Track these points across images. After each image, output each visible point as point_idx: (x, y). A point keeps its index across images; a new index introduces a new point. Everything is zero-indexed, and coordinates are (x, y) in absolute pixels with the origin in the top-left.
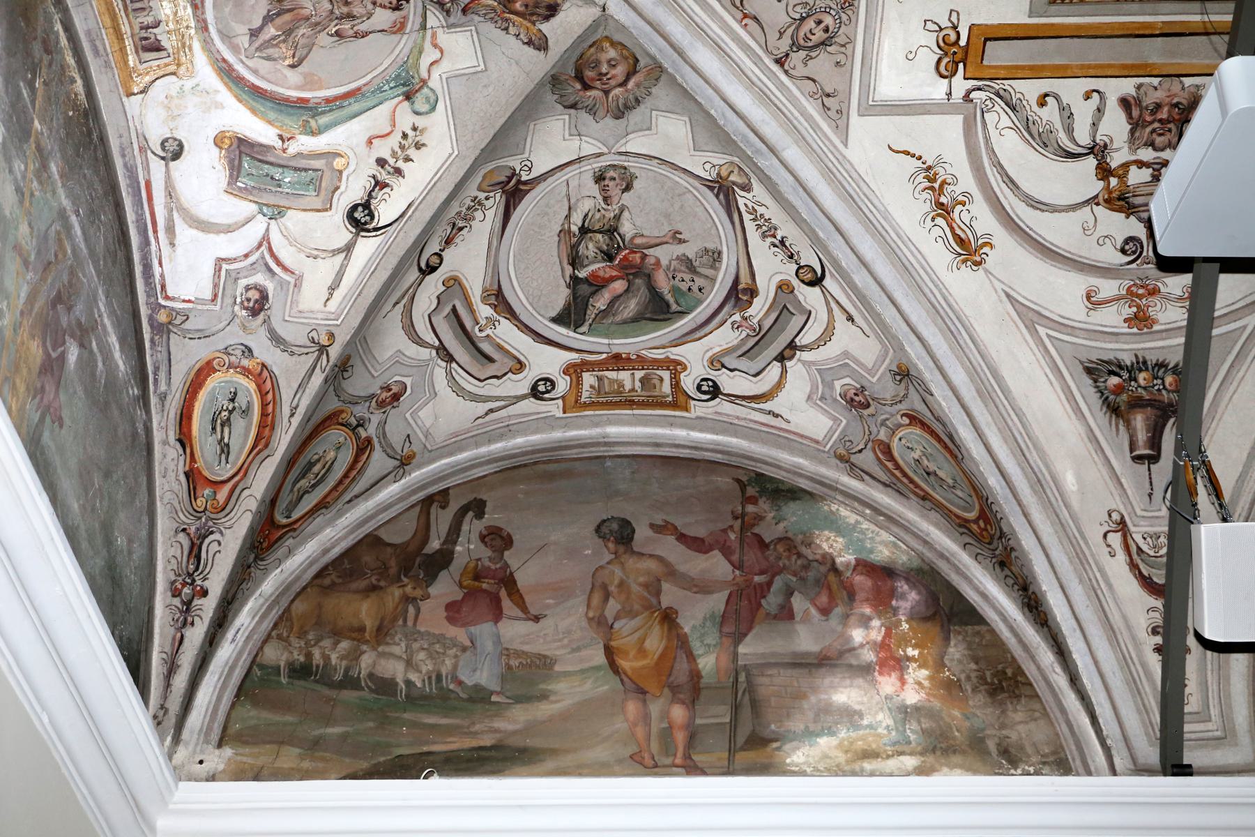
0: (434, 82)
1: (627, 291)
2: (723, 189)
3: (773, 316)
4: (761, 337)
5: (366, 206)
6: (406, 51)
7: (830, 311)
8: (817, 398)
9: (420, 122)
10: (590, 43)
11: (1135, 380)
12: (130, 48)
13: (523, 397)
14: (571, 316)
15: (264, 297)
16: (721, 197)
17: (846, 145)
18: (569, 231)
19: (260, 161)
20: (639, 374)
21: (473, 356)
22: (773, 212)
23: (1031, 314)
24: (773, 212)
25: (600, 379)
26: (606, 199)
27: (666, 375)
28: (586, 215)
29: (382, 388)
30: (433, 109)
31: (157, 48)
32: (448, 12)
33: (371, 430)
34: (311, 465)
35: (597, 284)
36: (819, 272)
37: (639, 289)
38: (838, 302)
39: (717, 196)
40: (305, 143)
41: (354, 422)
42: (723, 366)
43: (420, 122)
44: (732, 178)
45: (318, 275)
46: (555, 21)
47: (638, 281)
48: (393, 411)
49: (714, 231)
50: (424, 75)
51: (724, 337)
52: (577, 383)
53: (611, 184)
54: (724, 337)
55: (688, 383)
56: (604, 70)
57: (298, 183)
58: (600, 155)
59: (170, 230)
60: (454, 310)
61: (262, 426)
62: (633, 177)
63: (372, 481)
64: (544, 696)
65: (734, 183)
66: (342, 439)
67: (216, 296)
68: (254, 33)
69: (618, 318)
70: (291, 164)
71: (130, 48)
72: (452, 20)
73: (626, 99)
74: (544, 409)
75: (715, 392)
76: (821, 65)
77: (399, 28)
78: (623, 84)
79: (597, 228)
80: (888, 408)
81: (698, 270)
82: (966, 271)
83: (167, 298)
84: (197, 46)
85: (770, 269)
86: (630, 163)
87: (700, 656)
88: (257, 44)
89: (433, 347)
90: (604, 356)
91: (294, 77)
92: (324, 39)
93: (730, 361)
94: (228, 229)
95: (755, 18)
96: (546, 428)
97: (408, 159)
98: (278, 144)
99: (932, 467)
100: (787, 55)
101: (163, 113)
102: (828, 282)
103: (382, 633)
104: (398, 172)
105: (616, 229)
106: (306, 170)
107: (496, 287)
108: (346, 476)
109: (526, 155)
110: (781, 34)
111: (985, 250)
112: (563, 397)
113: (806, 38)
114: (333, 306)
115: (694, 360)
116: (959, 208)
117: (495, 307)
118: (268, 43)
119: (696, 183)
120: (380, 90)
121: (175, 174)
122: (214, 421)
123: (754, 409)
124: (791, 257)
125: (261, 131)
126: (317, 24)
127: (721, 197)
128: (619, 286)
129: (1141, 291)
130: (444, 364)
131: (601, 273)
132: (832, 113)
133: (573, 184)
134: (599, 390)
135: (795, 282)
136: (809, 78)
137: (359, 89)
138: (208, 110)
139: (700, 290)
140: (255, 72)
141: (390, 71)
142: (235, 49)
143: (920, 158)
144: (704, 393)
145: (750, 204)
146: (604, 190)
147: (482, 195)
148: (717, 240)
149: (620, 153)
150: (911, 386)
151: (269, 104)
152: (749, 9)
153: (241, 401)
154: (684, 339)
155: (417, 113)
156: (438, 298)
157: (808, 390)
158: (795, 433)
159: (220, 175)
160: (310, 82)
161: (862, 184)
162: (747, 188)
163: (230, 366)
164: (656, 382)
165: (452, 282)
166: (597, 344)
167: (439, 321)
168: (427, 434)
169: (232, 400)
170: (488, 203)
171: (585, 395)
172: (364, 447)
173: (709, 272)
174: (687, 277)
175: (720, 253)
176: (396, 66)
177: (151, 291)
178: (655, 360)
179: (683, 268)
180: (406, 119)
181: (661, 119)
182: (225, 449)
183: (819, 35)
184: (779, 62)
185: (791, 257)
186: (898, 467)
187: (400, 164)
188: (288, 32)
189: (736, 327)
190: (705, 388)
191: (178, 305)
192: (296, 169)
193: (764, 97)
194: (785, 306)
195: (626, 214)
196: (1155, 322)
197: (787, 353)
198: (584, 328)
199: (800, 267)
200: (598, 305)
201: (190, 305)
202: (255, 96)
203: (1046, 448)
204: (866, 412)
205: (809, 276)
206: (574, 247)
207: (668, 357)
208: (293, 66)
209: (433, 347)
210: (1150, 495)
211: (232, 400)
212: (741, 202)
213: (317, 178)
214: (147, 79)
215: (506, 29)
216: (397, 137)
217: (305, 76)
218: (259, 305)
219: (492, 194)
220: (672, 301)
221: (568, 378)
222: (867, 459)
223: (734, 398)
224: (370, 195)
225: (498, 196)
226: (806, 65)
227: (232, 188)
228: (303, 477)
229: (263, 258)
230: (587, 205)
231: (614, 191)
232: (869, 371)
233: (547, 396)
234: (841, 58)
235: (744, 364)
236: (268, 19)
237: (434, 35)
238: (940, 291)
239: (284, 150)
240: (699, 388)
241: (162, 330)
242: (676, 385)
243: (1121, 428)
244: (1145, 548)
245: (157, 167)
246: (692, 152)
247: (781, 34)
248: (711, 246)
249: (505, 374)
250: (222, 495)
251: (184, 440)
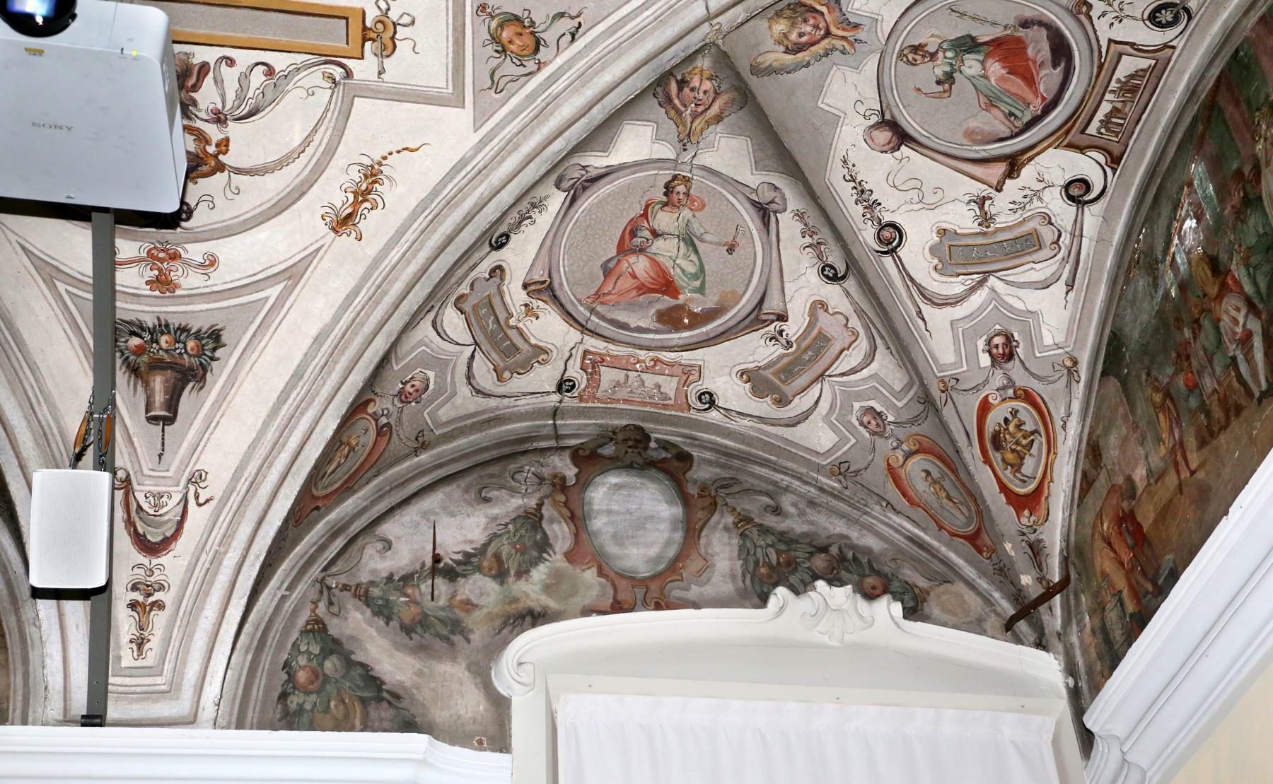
11: (157, 342)
129: (162, 255)
196: (177, 286)
203: (58, 404)
210: (160, 456)
243: (140, 388)
244: (145, 506)
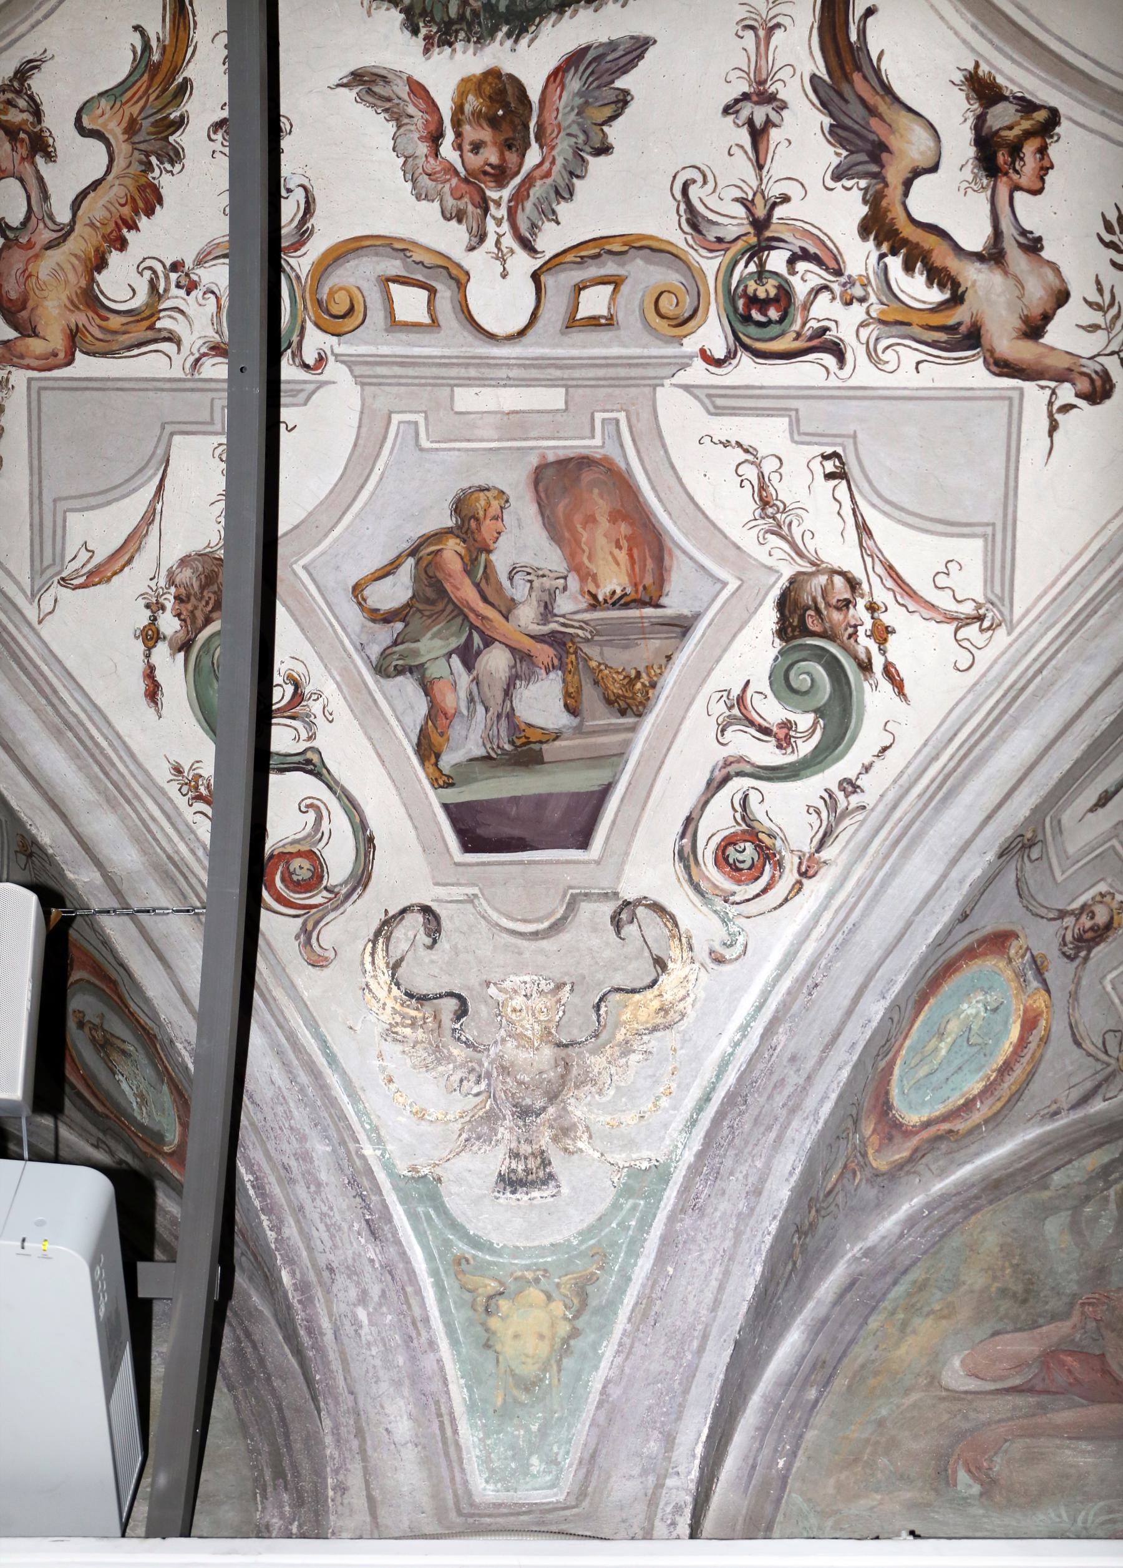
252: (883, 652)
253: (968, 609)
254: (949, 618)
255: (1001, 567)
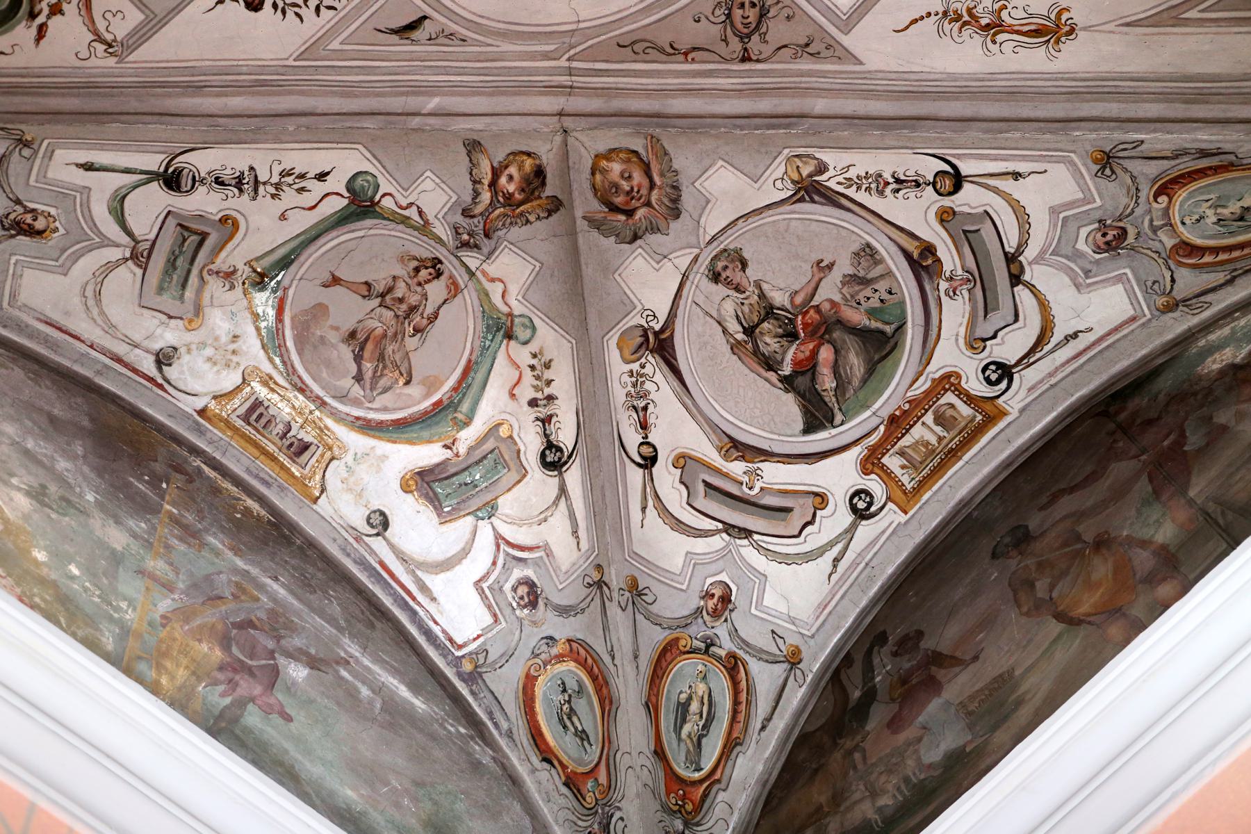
0: (518, 309)
1: (837, 352)
2: (810, 190)
3: (967, 250)
4: (980, 279)
5: (550, 446)
6: (476, 302)
7: (996, 191)
8: (1084, 279)
9: (534, 347)
10: (589, 171)
12: (287, 462)
13: (852, 530)
14: (817, 416)
15: (531, 585)
16: (816, 198)
17: (861, 63)
18: (739, 342)
19: (446, 478)
20: (929, 418)
21: (765, 517)
22: (864, 162)
23: (1165, 15)
24: (864, 162)
25: (902, 453)
26: (738, 289)
27: (950, 398)
28: (737, 316)
29: (702, 598)
30: (534, 329)
31: (305, 447)
32: (476, 246)
33: (726, 645)
34: (683, 708)
35: (807, 367)
36: (948, 168)
37: (844, 341)
38: (992, 175)
39: (813, 201)
40: (467, 437)
41: (703, 646)
42: (984, 340)
43: (534, 347)
44: (805, 173)
45: (556, 533)
46: (549, 176)
47: (836, 335)
48: (733, 615)
49: (844, 233)
50: (505, 309)
51: (955, 314)
52: (887, 475)
53: (728, 273)
54: (955, 314)
55: (976, 386)
56: (628, 188)
57: (488, 472)
58: (696, 259)
59: (424, 588)
60: (707, 484)
61: (598, 691)
62: (738, 251)
63: (773, 696)
64: (1019, 703)
65: (810, 175)
66: (700, 667)
67: (495, 615)
68: (359, 378)
69: (856, 382)
70: (470, 462)
71: (287, 462)
72: (485, 250)
73: (667, 195)
74: (884, 524)
75: (1004, 372)
76: (777, 30)
77: (454, 290)
78: (652, 185)
79: (756, 319)
80: (1138, 211)
81: (870, 276)
82: (1068, 46)
83: (460, 647)
84: (329, 422)
85: (917, 214)
86: (727, 242)
87: (1153, 536)
88: (368, 386)
89: (718, 531)
90: (882, 428)
91: (414, 390)
92: (411, 343)
93: (985, 329)
94: (465, 553)
95: (694, 49)
96: (893, 536)
97: (549, 383)
98: (448, 454)
99: (1234, 207)
100: (746, 49)
101: (348, 497)
102: (966, 168)
103: (838, 799)
104: (550, 398)
105: (772, 307)
106: (485, 457)
107: (726, 440)
108: (736, 702)
109: (639, 307)
110: (725, 40)
111: (1064, 17)
112: (889, 499)
113: (746, 25)
114: (584, 545)
115: (951, 355)
116: (1004, 14)
117: (743, 458)
118: (376, 378)
119: (787, 208)
120: (484, 349)
121: (395, 540)
122: (561, 720)
123: (1052, 351)
124: (918, 185)
125: (429, 454)
126: (396, 334)
127: (816, 198)
128: (826, 353)
130: (745, 542)
131: (801, 356)
132: (825, 53)
133: (700, 300)
134: (911, 465)
135: (947, 202)
136: (779, 48)
137: (469, 361)
138: (379, 470)
139: (890, 293)
140: (385, 409)
141: (479, 328)
142: (356, 403)
143: (929, 14)
144: (998, 381)
145: (840, 179)
146: (728, 283)
147: (635, 367)
148: (854, 237)
149: (709, 243)
150: (1126, 163)
151: (417, 427)
152: (683, 47)
153: (572, 685)
154: (928, 350)
155: (526, 343)
156: (682, 482)
157: (1067, 280)
158: (1109, 334)
159: (427, 514)
160: (431, 385)
161: (906, 76)
162: (822, 168)
163: (545, 665)
164: (950, 412)
165: (682, 461)
166: (864, 422)
167: (701, 503)
168: (792, 621)
169: (564, 691)
170: (649, 370)
171: (905, 479)
172: (733, 665)
173: (878, 271)
174: (868, 292)
175: (868, 245)
176: (479, 320)
177: (445, 652)
178: (927, 393)
179: (857, 288)
180: (523, 355)
181: (705, 184)
182: (582, 736)
183: (752, 14)
184: (745, 59)
185: (918, 185)
186: (1215, 250)
187: (547, 391)
188: (381, 358)
189: (953, 293)
190: (994, 377)
191: (472, 647)
192: (478, 463)
193: (758, 92)
194: (965, 232)
195: (765, 286)
197: (1014, 270)
198: (839, 418)
199: (934, 184)
200: (827, 386)
201: (481, 640)
202: (400, 429)
204: (1131, 239)
205: (948, 183)
206: (756, 352)
207: (934, 380)
208: (408, 383)
209: (718, 531)
211: (564, 691)
212: (832, 184)
213: (496, 456)
214: (318, 477)
215: (528, 221)
216: (528, 374)
217: (423, 382)
218: (532, 595)
219: (643, 360)
220: (879, 325)
221: (873, 476)
222: (1188, 281)
223: (1027, 359)
224: (546, 436)
225: (650, 358)
226: (766, 42)
227: (445, 518)
228: (684, 721)
229: (508, 554)
230: (729, 308)
231: (737, 277)
232: (1088, 200)
233: (873, 509)
234: (785, 12)
235: (996, 320)
236: (358, 358)
237: (484, 273)
238: (1062, 79)
239: (457, 455)
240: (988, 381)
241: (472, 678)
242: (970, 399)
245: (378, 544)
246: (756, 186)
247: (725, 40)
248: (856, 247)
249: (814, 515)
250: (603, 778)
251: (548, 757)
252: (48, 17)
253: (109, 37)
254: (96, 32)
255: (141, 35)
